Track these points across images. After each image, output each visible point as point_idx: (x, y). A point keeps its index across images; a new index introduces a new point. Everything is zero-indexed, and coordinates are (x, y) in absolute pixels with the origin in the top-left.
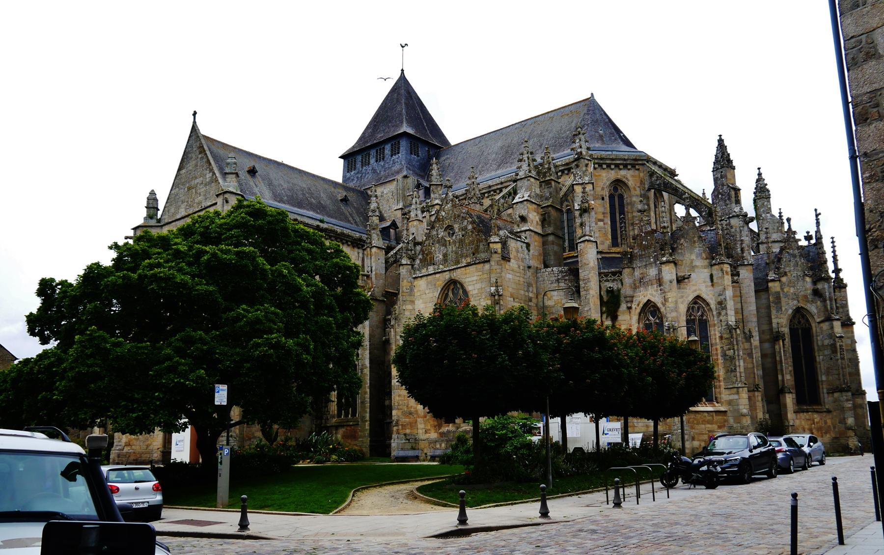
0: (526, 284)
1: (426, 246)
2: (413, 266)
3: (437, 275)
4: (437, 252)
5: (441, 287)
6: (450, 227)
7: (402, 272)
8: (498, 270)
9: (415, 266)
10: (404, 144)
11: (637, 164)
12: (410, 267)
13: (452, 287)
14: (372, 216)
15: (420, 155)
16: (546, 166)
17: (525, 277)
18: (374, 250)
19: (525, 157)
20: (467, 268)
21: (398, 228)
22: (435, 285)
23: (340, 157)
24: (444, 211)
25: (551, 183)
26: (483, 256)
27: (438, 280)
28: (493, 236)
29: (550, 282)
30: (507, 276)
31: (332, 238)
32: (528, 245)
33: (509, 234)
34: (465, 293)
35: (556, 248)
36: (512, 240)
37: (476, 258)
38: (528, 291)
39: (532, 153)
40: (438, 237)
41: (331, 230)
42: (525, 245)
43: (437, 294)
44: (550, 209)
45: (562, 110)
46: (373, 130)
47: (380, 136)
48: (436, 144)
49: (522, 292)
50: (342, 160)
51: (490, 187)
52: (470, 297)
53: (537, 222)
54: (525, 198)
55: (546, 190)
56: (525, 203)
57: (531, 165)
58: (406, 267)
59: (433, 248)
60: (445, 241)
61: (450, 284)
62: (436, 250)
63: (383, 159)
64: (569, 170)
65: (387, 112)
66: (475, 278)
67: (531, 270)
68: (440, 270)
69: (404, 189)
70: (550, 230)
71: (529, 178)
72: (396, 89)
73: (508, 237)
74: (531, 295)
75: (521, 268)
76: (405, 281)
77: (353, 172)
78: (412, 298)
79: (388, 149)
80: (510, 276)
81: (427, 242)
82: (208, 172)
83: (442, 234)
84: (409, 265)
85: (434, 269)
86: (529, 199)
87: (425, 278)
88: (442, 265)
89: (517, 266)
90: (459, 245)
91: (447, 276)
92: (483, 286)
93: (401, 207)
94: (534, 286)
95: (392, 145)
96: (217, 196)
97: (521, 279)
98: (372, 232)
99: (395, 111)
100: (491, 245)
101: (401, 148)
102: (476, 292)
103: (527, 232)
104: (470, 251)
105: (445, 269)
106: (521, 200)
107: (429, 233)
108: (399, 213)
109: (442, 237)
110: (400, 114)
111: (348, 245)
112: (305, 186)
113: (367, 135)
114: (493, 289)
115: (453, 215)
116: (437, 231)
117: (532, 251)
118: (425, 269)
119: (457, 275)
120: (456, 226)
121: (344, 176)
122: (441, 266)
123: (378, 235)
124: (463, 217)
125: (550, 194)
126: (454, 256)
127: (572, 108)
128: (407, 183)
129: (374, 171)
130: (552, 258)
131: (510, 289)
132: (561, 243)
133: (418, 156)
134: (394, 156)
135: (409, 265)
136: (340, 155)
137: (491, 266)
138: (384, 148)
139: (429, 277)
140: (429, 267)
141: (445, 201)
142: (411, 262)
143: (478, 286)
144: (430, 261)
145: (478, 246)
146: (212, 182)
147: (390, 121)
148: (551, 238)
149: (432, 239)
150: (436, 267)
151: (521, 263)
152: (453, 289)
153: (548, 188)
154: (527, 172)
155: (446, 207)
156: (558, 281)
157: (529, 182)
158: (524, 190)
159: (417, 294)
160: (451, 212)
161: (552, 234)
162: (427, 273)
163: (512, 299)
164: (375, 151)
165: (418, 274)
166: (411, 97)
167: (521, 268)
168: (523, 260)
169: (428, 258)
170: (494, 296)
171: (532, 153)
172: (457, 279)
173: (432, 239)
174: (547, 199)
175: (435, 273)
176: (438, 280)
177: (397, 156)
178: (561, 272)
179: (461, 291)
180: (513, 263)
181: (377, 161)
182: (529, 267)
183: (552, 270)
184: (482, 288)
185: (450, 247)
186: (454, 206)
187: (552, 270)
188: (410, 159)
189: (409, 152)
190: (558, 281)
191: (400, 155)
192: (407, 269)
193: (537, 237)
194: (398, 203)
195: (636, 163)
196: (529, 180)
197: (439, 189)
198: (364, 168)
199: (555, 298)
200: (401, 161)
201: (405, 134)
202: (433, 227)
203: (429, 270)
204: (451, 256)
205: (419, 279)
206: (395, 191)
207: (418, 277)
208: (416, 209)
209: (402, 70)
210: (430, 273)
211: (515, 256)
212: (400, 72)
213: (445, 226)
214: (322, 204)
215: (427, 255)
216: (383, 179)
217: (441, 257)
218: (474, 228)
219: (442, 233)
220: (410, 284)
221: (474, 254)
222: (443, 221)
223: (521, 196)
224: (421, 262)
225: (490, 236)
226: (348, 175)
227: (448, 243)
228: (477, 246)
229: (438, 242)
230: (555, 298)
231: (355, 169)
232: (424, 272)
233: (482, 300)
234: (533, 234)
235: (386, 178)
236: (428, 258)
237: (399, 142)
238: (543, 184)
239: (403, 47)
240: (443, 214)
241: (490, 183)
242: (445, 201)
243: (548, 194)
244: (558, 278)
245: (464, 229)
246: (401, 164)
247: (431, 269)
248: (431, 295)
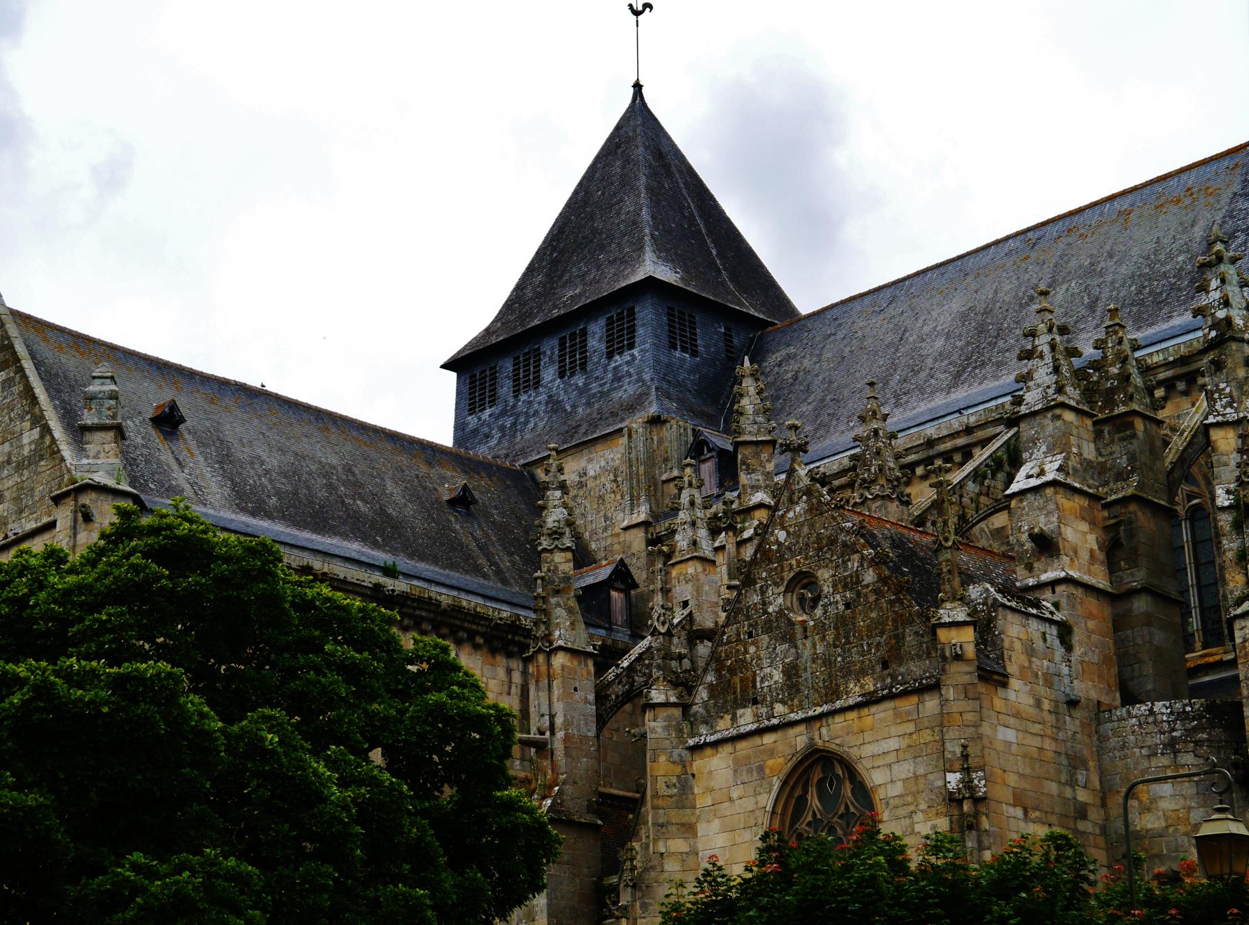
0: (1064, 761)
1: (729, 642)
2: (685, 708)
3: (768, 739)
4: (766, 662)
5: (782, 776)
6: (803, 582)
7: (653, 730)
8: (969, 717)
9: (695, 708)
10: (647, 318)
12: (677, 712)
13: (817, 775)
14: (551, 551)
15: (701, 349)
16: (1114, 370)
17: (1061, 735)
18: (559, 660)
19: (1043, 342)
20: (865, 711)
21: (636, 586)
22: (761, 769)
23: (443, 367)
24: (783, 528)
25: (1131, 425)
26: (917, 669)
27: (771, 753)
28: (948, 605)
29: (1144, 752)
30: (1000, 736)
31: (425, 626)
32: (1065, 632)
33: (999, 597)
34: (863, 793)
35: (1159, 637)
36: (1011, 617)
37: (894, 677)
38: (1072, 783)
39: (1063, 330)
40: (766, 612)
41: (420, 600)
42: (1054, 630)
43: (767, 800)
44: (1133, 507)
45: (1158, 188)
46: (548, 275)
47: (572, 295)
48: (752, 312)
49: (1053, 788)
50: (453, 376)
51: (930, 443)
52: (879, 807)
53: (1092, 551)
54: (1050, 477)
55: (1116, 448)
56: (1049, 491)
57: (1064, 369)
58: (663, 713)
59: (752, 649)
60: (791, 623)
61: (810, 767)
62: (763, 654)
63: (583, 366)
64: (1191, 379)
65: (592, 217)
66: (893, 744)
67: (1079, 713)
68: (775, 721)
69: (650, 461)
70: (1136, 578)
71: (1058, 411)
72: (618, 146)
73: (996, 605)
74: (1082, 796)
75: (1046, 705)
76: (662, 759)
77: (488, 412)
79: (596, 333)
80: (1010, 735)
81: (731, 631)
82: (27, 425)
83: (777, 601)
84: (674, 705)
85: (757, 717)
86: (1061, 477)
87: (728, 748)
88: (783, 702)
89: (1031, 701)
90: (837, 637)
91: (799, 739)
92: (921, 771)
93: (642, 517)
94: (1091, 764)
95: (610, 322)
96: (57, 500)
97: (1048, 745)
98: (553, 600)
99: (618, 214)
100: (943, 634)
101: (640, 331)
102: (898, 789)
103: (1059, 589)
104: (874, 655)
105: (793, 716)
106: (1034, 482)
107: (738, 600)
108: (637, 540)
109: (780, 612)
110: (634, 223)
111: (476, 647)
112: (334, 461)
113: (529, 293)
114: (953, 779)
115: (813, 539)
116: (763, 592)
117: (1078, 651)
118: (728, 717)
119: (834, 734)
120: (824, 575)
121: (459, 427)
122: (779, 708)
123: (570, 611)
124: (845, 545)
125: (1132, 458)
126: (820, 672)
127: (1190, 179)
128: (661, 441)
129: (554, 405)
130: (1149, 669)
131: (1012, 780)
132: (1178, 619)
133: (694, 353)
134: (617, 357)
135: (674, 705)
136: (445, 358)
137: (944, 702)
138: (584, 333)
139: (742, 745)
140: (740, 712)
141: (786, 494)
142: (680, 697)
143: (905, 769)
144: (744, 689)
145: (899, 638)
146: (41, 458)
147: (602, 248)
148: (1141, 605)
149: (748, 617)
150: (763, 710)
151: (1042, 690)
152: (820, 783)
153: (1122, 439)
154: (1051, 391)
155: (791, 514)
156: (1172, 746)
157: (1058, 423)
158: (1044, 448)
159: (703, 801)
160: (806, 529)
161: (1145, 590)
162: (733, 732)
163: (1019, 812)
164: (555, 342)
165: (707, 736)
166: (667, 167)
167: (1046, 705)
168: (1050, 680)
169: (737, 680)
170: (960, 802)
171: (1063, 330)
172: (833, 747)
173: (748, 617)
174: (1121, 476)
175: (760, 732)
176: (771, 753)
177: (626, 357)
178: (1182, 716)
179: (847, 789)
180: (1018, 693)
181: (562, 374)
182: (1073, 703)
183: (1151, 711)
184: (916, 777)
185: (808, 643)
186: (815, 509)
187: (1151, 711)
188: (669, 365)
189: (665, 341)
190: (1172, 746)
191: (635, 352)
192: (668, 719)
193: (1092, 604)
194: (632, 505)
196: (1059, 417)
197: (764, 456)
198: (524, 397)
199: (1165, 805)
200: (639, 373)
201: (651, 284)
202: (749, 582)
203: (741, 721)
204: (813, 673)
205: (709, 751)
206: (623, 468)
207: (706, 745)
208: (693, 524)
209: (638, 87)
210: (742, 730)
211: (1022, 668)
212: (632, 90)
213: (787, 576)
214: (389, 516)
215: (732, 671)
216: (582, 430)
217: (778, 676)
218: (882, 580)
219: (780, 600)
220: (678, 770)
221: (885, 665)
222: (781, 559)
223: (1036, 471)
224: (711, 697)
225: (938, 604)
226: (472, 421)
227: (799, 629)
228: (896, 637)
229: (768, 629)
230: (1165, 805)
231: (492, 403)
232: (724, 726)
233: (919, 817)
234: (1079, 592)
235: (594, 425)
236: (737, 680)
237: (632, 313)
238: (1106, 429)
239: (637, 13)
240: (782, 535)
241: (931, 431)
242: (786, 494)
243: (1123, 462)
244: (1174, 738)
245: (852, 583)
246: (640, 379)
247: (747, 719)
248: (748, 804)
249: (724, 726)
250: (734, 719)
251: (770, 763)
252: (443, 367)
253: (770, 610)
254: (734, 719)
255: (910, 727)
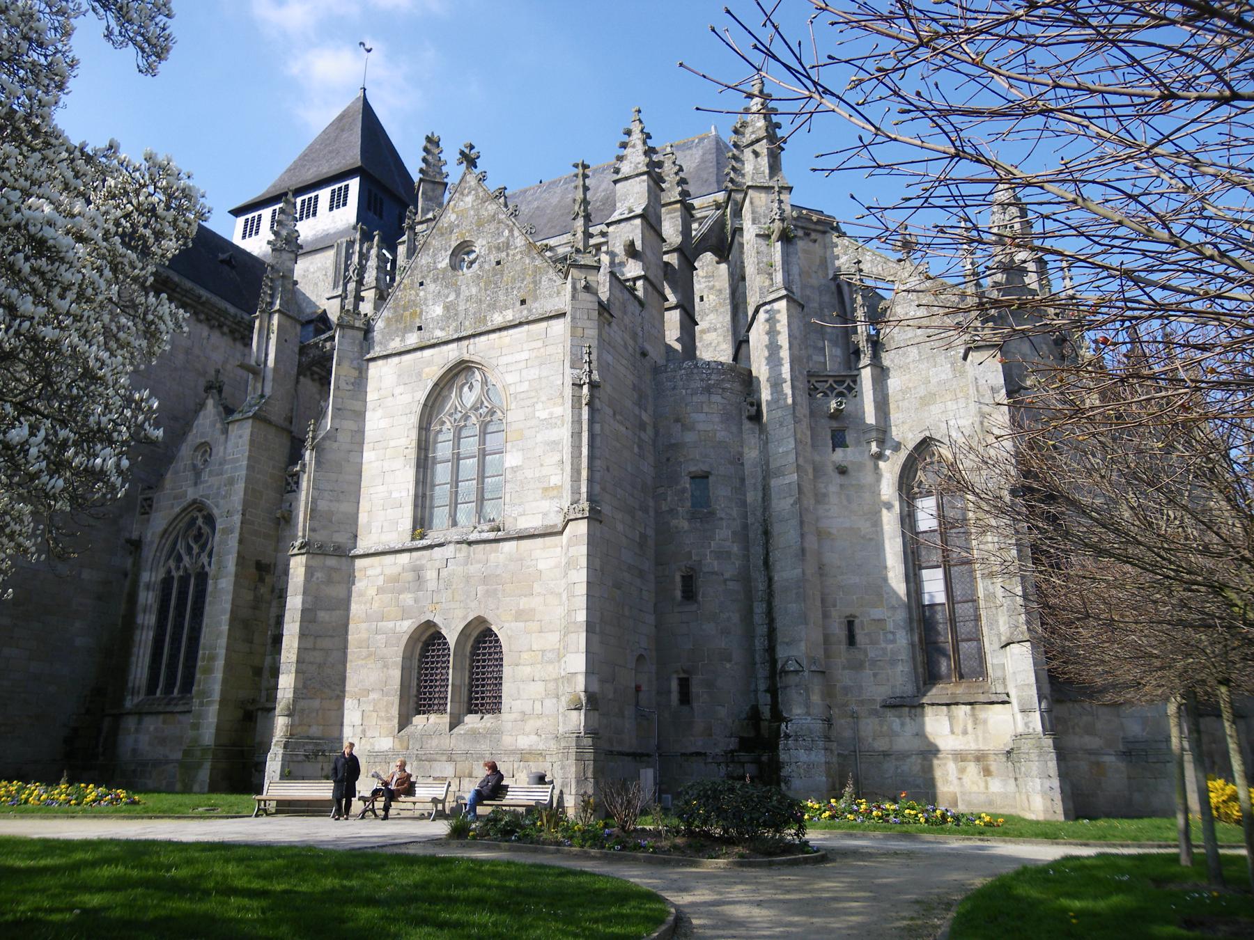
11: (815, 231)
12: (360, 335)
22: (419, 374)
23: (230, 212)
37: (530, 311)
59: (422, 294)
66: (525, 355)
78: (356, 405)
91: (451, 354)
118: (398, 339)
119: (477, 349)
120: (480, 246)
163: (611, 413)
176: (429, 363)
184: (540, 378)
195: (813, 227)
221: (523, 302)
228: (535, 282)
236: (407, 313)
249: (395, 345)
250: (403, 340)
251: (427, 370)
252: (230, 212)
253: (439, 266)
254: (403, 340)
255: (540, 344)
